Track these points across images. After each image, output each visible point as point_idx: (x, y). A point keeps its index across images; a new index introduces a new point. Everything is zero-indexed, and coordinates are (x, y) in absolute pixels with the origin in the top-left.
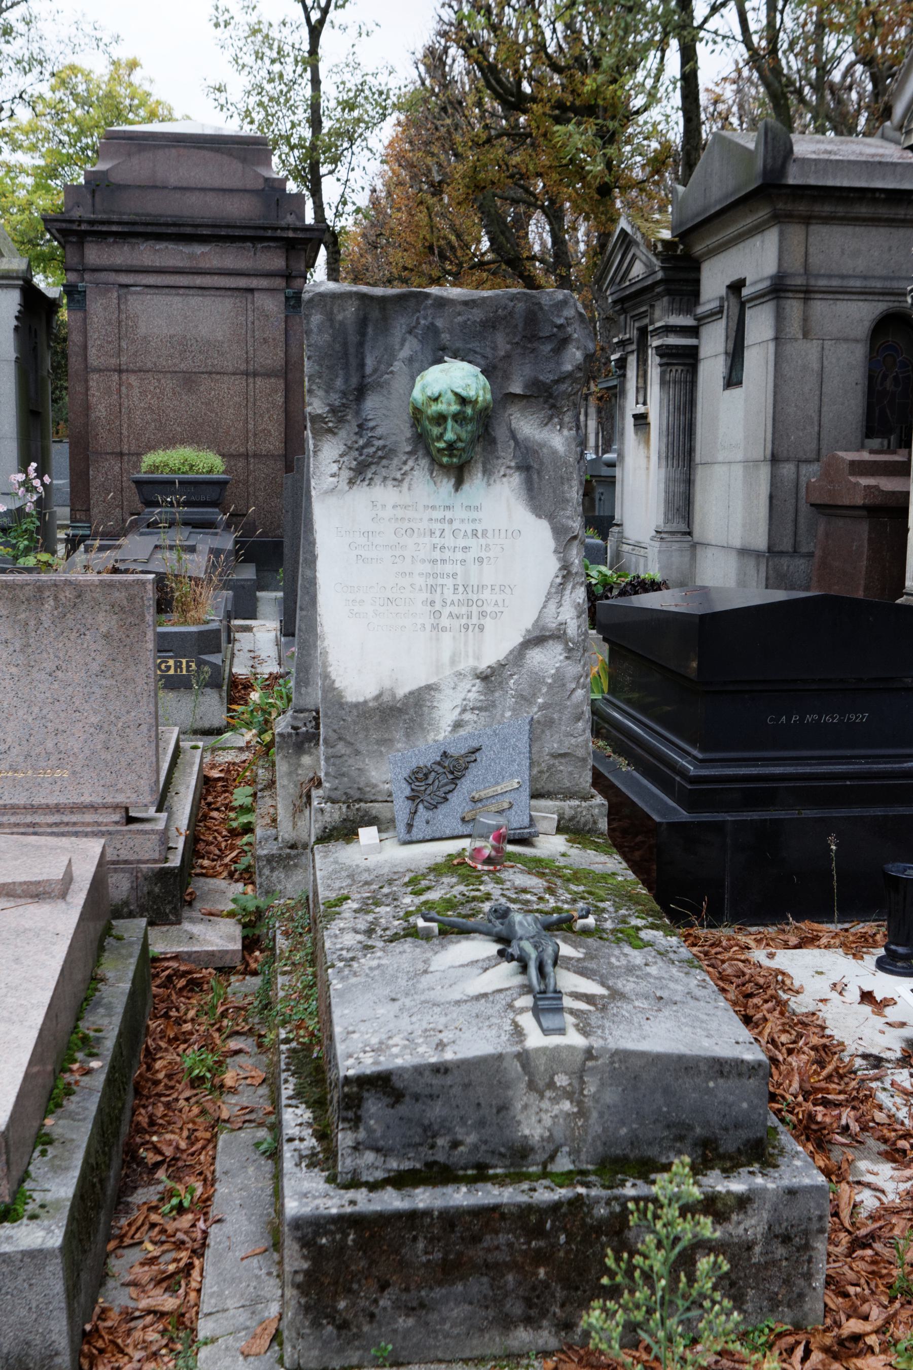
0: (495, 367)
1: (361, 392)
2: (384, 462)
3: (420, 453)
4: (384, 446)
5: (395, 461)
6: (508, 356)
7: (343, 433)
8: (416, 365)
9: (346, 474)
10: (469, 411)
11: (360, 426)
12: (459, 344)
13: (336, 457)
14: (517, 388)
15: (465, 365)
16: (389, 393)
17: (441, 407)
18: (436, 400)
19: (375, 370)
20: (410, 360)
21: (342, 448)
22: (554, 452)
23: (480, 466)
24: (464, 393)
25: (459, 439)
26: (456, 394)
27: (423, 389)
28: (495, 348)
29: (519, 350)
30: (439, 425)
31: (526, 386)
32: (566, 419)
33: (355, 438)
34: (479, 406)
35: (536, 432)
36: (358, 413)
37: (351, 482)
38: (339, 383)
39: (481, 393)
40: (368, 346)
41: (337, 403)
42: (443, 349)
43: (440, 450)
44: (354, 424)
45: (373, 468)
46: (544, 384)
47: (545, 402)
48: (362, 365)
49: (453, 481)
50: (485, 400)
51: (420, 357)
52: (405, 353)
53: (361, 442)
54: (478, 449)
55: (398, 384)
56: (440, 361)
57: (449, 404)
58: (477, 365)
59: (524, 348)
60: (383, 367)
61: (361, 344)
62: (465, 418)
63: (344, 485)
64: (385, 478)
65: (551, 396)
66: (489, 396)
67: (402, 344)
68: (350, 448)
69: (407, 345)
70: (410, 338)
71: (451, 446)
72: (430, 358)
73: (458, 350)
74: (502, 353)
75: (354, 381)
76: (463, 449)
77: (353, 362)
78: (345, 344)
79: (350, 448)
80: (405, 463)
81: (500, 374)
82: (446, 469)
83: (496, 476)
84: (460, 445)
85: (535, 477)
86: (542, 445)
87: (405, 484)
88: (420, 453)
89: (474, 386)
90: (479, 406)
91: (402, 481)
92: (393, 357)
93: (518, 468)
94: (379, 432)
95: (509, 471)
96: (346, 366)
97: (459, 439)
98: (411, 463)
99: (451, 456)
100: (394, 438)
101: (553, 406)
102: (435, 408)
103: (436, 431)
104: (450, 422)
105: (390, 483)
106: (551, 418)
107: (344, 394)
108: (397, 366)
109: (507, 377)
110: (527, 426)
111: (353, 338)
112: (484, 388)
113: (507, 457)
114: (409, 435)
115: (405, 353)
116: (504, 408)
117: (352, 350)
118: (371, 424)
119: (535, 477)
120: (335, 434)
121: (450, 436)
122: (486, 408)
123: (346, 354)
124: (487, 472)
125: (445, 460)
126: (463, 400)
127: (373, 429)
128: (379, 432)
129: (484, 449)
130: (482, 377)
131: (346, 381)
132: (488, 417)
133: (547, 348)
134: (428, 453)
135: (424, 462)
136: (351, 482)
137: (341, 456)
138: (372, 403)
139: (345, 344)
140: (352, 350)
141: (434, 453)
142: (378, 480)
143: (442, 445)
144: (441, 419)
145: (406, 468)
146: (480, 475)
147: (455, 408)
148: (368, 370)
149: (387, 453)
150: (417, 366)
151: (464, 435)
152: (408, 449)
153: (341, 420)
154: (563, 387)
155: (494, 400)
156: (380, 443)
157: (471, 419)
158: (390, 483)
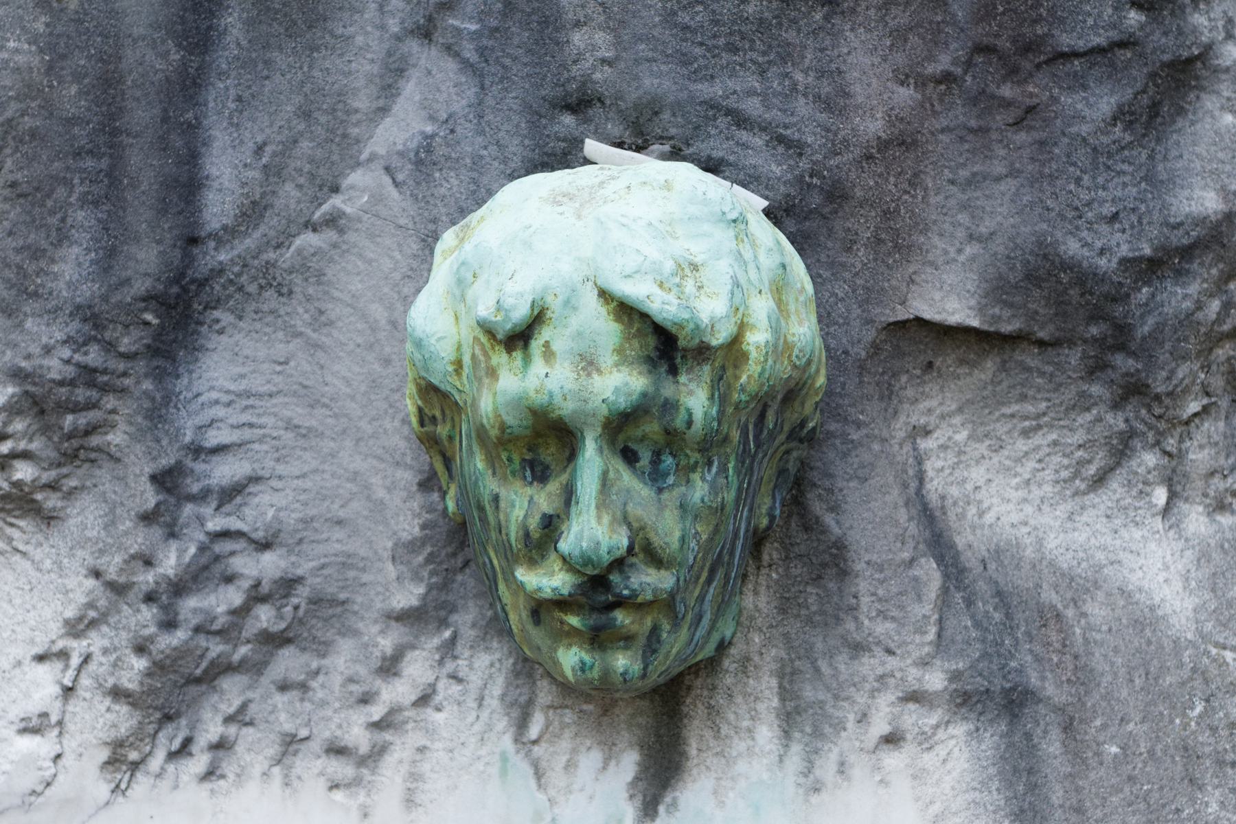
0: (837, 195)
1: (178, 315)
2: (288, 662)
3: (466, 619)
4: (288, 584)
5: (343, 659)
6: (901, 142)
7: (85, 516)
8: (451, 184)
9: (95, 720)
10: (695, 398)
11: (167, 480)
12: (656, 81)
13: (51, 634)
14: (949, 296)
15: (686, 173)
16: (320, 320)
17: (544, 379)
18: (519, 339)
19: (253, 212)
20: (423, 161)
21: (82, 588)
22: (1144, 620)
23: (766, 685)
24: (664, 306)
25: (644, 549)
26: (627, 312)
27: (461, 285)
28: (835, 103)
29: (959, 114)
30: (539, 473)
31: (997, 290)
32: (1199, 456)
33: (139, 539)
34: (750, 375)
35: (1052, 519)
36: (158, 414)
37: (122, 761)
38: (71, 271)
39: (761, 308)
40: (220, 94)
41: (55, 367)
42: (581, 103)
43: (540, 609)
44: (140, 467)
45: (232, 692)
46: (1084, 278)
47: (1095, 368)
48: (186, 186)
49: (629, 763)
50: (780, 347)
51: (470, 143)
52: (399, 130)
53: (171, 562)
54: (757, 600)
55: (357, 276)
56: (565, 156)
57: (588, 364)
58: (749, 181)
59: (982, 100)
60: (289, 195)
61: (188, 86)
62: (672, 440)
63: (85, 775)
64: (291, 744)
65: (1120, 338)
66: (804, 330)
67: (388, 90)
68: (118, 589)
69: (411, 89)
70: (424, 56)
71: (598, 587)
72: (516, 149)
73: (653, 107)
74: (873, 126)
75: (146, 261)
76: (668, 604)
77: (144, 167)
78: (107, 85)
79: (118, 589)
80: (390, 667)
81: (864, 225)
82: (595, 701)
83: (851, 742)
84: (649, 580)
85: (1052, 746)
86: (1080, 587)
87: (391, 775)
88: (466, 619)
89: (720, 272)
90: (750, 375)
91: (378, 752)
92: (342, 148)
93: (965, 700)
94: (259, 511)
95: (914, 719)
96: (110, 191)
97: (644, 549)
98: (418, 668)
99: (599, 638)
100: (337, 542)
101: (1133, 391)
102: (513, 385)
103: (521, 504)
104: (592, 460)
105: (312, 767)
106: (1121, 448)
107: (92, 321)
108: (362, 188)
109: (897, 242)
110: (1002, 483)
111: (149, 59)
112: (779, 288)
113: (903, 643)
114: (409, 527)
115: (399, 130)
116: (888, 394)
117: (141, 115)
118: (225, 471)
119: (1052, 746)
120: (49, 519)
121: (591, 531)
122: (792, 393)
123: (110, 132)
124: (801, 719)
125: (570, 658)
126: (663, 345)
127: (231, 494)
128: (259, 511)
129: (786, 605)
130: (767, 234)
131: (108, 258)
132: (803, 436)
133: (1095, 105)
134: (496, 626)
135: (485, 666)
136: (122, 761)
137: (77, 627)
138: (229, 369)
139: (107, 85)
140: (141, 115)
141: (517, 618)
142: (254, 750)
143: (550, 580)
144: (544, 441)
145: (397, 692)
146: (766, 734)
147: (619, 383)
148: (218, 208)
149: (299, 619)
150: (446, 184)
151: (669, 530)
152: (408, 596)
153: (78, 451)
154: (1179, 296)
155: (836, 358)
156: (270, 565)
157: (710, 445)
158: (312, 767)
